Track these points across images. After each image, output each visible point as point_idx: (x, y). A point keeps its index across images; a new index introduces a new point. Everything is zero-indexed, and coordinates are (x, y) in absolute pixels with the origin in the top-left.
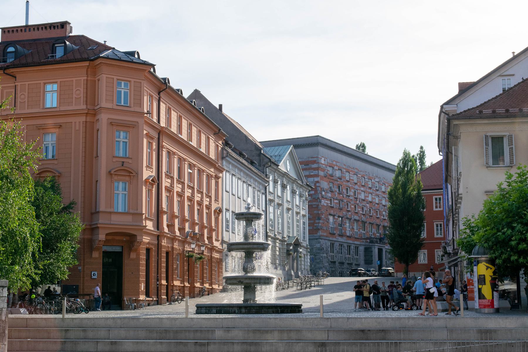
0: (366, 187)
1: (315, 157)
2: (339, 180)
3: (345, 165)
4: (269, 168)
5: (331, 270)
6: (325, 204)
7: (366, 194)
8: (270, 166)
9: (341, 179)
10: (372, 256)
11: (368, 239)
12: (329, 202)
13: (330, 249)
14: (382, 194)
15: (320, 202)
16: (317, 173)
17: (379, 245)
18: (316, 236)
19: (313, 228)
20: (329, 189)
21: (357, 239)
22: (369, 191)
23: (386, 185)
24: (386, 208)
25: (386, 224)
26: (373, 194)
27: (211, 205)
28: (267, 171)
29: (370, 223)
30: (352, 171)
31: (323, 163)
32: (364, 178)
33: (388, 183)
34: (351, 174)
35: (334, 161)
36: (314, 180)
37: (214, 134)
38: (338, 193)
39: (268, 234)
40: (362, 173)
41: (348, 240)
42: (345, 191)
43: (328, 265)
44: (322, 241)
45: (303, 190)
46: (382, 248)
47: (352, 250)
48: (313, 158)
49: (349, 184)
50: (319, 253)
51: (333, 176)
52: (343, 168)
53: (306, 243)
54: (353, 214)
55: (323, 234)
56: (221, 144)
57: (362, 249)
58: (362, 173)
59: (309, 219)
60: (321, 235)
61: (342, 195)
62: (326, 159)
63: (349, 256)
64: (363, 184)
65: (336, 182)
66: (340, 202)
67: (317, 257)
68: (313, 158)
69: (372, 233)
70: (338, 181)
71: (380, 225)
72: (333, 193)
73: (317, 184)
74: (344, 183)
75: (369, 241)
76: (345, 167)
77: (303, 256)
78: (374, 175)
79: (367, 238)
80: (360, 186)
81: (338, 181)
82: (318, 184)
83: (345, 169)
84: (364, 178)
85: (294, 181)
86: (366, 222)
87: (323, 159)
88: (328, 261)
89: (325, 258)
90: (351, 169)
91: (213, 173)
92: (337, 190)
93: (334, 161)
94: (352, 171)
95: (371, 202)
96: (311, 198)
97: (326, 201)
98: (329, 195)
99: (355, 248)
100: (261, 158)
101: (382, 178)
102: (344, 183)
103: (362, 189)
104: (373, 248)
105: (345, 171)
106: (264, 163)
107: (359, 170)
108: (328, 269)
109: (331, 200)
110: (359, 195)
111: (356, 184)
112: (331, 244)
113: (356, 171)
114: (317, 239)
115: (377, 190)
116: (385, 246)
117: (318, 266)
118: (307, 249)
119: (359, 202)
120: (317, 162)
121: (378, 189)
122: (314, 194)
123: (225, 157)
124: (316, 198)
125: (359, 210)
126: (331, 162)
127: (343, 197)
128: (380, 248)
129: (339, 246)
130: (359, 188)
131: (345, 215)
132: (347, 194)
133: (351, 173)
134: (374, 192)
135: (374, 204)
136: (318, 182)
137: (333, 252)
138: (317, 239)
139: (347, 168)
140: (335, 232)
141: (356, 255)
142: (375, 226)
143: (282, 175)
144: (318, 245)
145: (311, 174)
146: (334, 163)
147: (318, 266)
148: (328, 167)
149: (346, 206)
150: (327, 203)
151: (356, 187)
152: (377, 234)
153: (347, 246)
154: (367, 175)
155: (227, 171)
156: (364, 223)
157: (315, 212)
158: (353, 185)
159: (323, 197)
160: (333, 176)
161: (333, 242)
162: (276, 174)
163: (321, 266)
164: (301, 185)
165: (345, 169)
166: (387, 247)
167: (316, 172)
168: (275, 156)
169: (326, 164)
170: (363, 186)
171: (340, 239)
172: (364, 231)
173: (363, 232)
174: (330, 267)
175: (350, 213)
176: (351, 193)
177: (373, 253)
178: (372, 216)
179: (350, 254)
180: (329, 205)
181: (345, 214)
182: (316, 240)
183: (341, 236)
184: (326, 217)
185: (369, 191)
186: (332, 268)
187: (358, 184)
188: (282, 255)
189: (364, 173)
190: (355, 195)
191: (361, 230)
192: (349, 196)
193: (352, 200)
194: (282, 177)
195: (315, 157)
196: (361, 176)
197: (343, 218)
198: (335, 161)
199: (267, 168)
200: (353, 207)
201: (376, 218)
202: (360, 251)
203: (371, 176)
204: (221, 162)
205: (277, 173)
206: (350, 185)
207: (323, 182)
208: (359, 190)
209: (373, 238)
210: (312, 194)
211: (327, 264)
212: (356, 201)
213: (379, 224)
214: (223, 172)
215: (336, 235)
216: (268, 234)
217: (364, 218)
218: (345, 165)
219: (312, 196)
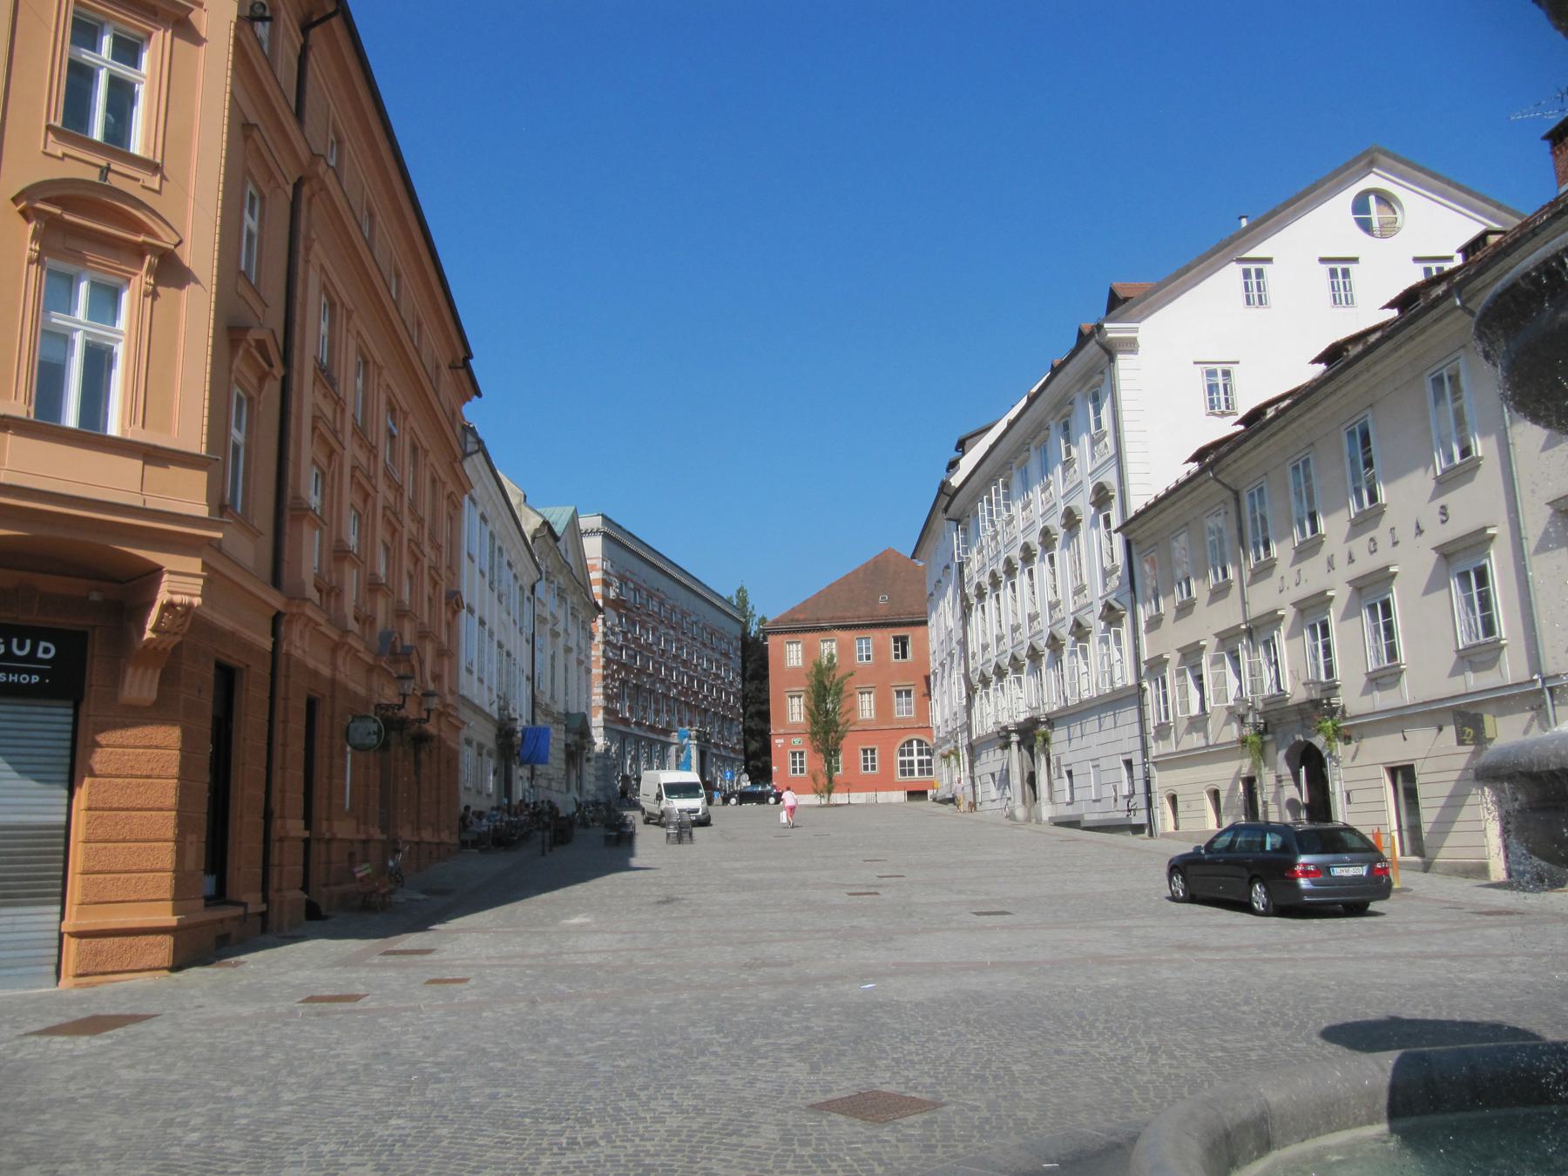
40: (671, 602)
52: (642, 587)
76: (645, 585)
94: (658, 597)
105: (645, 593)
113: (663, 596)
115: (695, 639)
146: (628, 574)
165: (646, 589)
203: (685, 608)
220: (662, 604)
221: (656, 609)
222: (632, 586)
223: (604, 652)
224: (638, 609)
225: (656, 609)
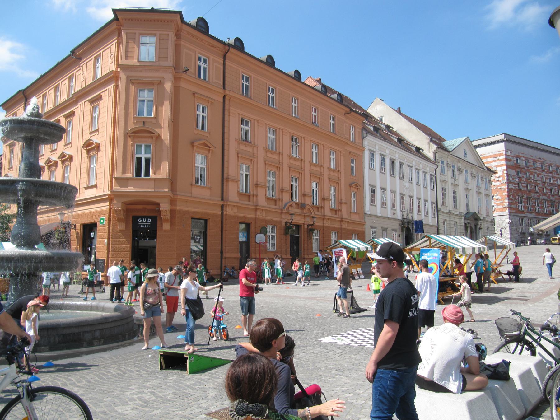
2: (526, 168)
3: (531, 156)
6: (513, 188)
12: (517, 186)
22: (557, 176)
38: (525, 179)
40: (549, 162)
51: (520, 165)
65: (523, 170)
66: (527, 185)
74: (531, 170)
76: (531, 158)
90: (537, 159)
92: (525, 176)
98: (517, 180)
102: (531, 170)
103: (550, 175)
109: (518, 184)
112: (520, 219)
125: (548, 191)
149: (534, 189)
150: (515, 187)
151: (544, 173)
156: (553, 202)
161: (522, 218)
165: (532, 159)
171: (529, 215)
172: (553, 208)
183: (530, 212)
185: (557, 176)
191: (550, 208)
193: (539, 184)
206: (538, 172)
208: (547, 176)
212: (544, 184)
215: (525, 211)
217: (552, 198)
218: (531, 156)
220: (542, 164)
222: (524, 159)
223: (508, 186)
224: (528, 167)
225: (539, 166)
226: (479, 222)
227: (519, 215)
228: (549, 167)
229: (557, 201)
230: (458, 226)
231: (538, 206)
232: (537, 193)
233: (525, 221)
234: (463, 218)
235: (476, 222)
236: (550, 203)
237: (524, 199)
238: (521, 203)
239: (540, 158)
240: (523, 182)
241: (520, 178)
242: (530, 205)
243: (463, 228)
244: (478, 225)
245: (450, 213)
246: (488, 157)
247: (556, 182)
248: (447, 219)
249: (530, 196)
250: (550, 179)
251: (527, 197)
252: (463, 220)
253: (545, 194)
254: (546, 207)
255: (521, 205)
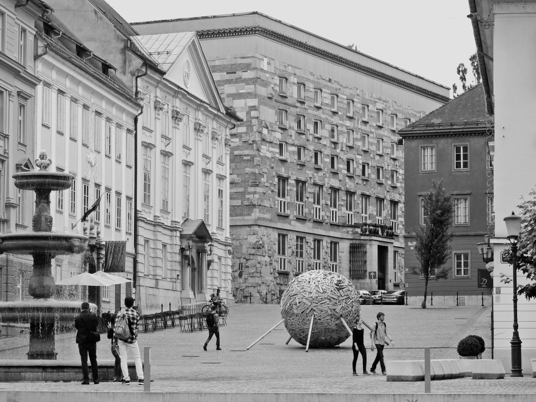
0: (356, 121)
1: (249, 57)
2: (298, 105)
3: (311, 74)
4: (144, 77)
5: (278, 289)
6: (269, 155)
7: (357, 134)
8: (145, 74)
9: (303, 103)
10: (365, 262)
11: (358, 227)
12: (277, 150)
13: (276, 246)
14: (390, 135)
15: (258, 150)
16: (253, 91)
17: (380, 239)
18: (248, 220)
19: (242, 203)
20: (278, 124)
21: (336, 227)
23: (400, 116)
24: (397, 163)
25: (397, 198)
26: (371, 135)
27: (8, 154)
28: (139, 84)
29: (363, 195)
30: (326, 87)
31: (265, 69)
32: (353, 101)
33: (403, 113)
34: (325, 92)
35: (288, 65)
36: (246, 104)
37: (17, 6)
39: (139, 215)
41: (317, 228)
42: (311, 127)
43: (273, 280)
44: (261, 231)
45: (220, 124)
46: (386, 245)
47: (323, 248)
48: (245, 58)
49: (319, 113)
50: (253, 254)
51: (286, 97)
52: (308, 80)
53: (224, 235)
54: (328, 175)
55: (262, 216)
56: (33, 27)
57: (344, 247)
58: (347, 90)
59: (231, 183)
60: (259, 219)
61: (304, 137)
62: (272, 62)
63: (318, 262)
64: (351, 115)
65: (292, 109)
67: (249, 263)
68: (245, 58)
69: (367, 216)
70: (297, 107)
71: (385, 197)
72: (286, 132)
73: (254, 113)
75: (359, 230)
76: (311, 78)
77: (216, 259)
78: (374, 95)
79: (356, 226)
80: (344, 117)
81: (297, 107)
82: (255, 112)
83: (313, 82)
84: (353, 101)
85: (199, 104)
86: (354, 193)
87: (266, 60)
88: (272, 271)
89: (266, 265)
91: (12, 88)
92: (295, 125)
93: (288, 65)
94: (326, 87)
95: (365, 152)
96: (240, 140)
97: (271, 149)
98: (278, 135)
99: (329, 245)
100: (127, 56)
101: (390, 101)
102: (309, 111)
103: (348, 123)
104: (368, 246)
106: (132, 68)
107: (341, 85)
108: (273, 288)
109: (281, 146)
110: (341, 136)
111: (335, 113)
114: (250, 226)
115: (380, 127)
116: (392, 241)
117: (251, 281)
118: (225, 245)
119: (342, 150)
120: (253, 66)
121: (380, 124)
122: (246, 133)
123: (41, 55)
124: (250, 142)
125: (341, 166)
126: (282, 68)
127: (308, 140)
128: (383, 245)
129: (297, 241)
130: (341, 122)
131: (310, 178)
132: (316, 135)
133: (324, 90)
134: (373, 130)
135: (372, 156)
136: (254, 108)
137: (284, 254)
138: (250, 226)
139: (316, 80)
140: (288, 212)
141: (331, 260)
142: (373, 200)
143: (173, 94)
144: (253, 239)
145: (241, 92)
146: (290, 69)
147: (251, 281)
148: (276, 78)
149: (313, 159)
151: (335, 120)
152: (377, 218)
153: (315, 240)
154: (358, 95)
155: (47, 85)
156: (350, 194)
157: (248, 170)
158: (330, 116)
159: (264, 140)
160: (286, 97)
161: (285, 232)
162: (158, 90)
163: (258, 280)
164: (215, 115)
165: (313, 82)
166: (396, 244)
167: (250, 88)
168: (159, 53)
169: (273, 71)
170: (351, 118)
173: (348, 212)
174: (277, 284)
175: (321, 174)
176: (323, 132)
177: (368, 254)
178: (367, 181)
179: (319, 258)
180: (278, 156)
181: (310, 176)
182: (247, 229)
183: (301, 220)
184: (270, 181)
185: (363, 127)
186: (282, 285)
187: (340, 113)
188: (169, 259)
189: (352, 92)
190: (333, 137)
191: (344, 209)
192: (319, 139)
194: (173, 96)
195: (249, 57)
196: (345, 97)
197: (307, 184)
198: (291, 66)
199: (138, 79)
200: (328, 160)
201: (376, 185)
202: (341, 250)
203: (367, 97)
204: (32, 65)
205: (161, 89)
206: (323, 116)
207: (266, 108)
208: (342, 125)
209: (369, 225)
210: (242, 133)
211: (269, 278)
212: (335, 148)
213: (382, 196)
214: (36, 85)
215: (291, 217)
216: (139, 215)
217: (350, 185)
218: (311, 74)
219: (241, 137)
220: (335, 95)
221: (328, 101)
224: (303, 103)
225: (328, 101)
226: (206, 245)
227: (279, 225)
228: (348, 104)
229: (359, 192)
230: (168, 255)
231: (318, 203)
232: (319, 169)
233: (291, 241)
234: (178, 234)
235: (200, 244)
236: (344, 198)
237: (291, 184)
238: (284, 196)
239: (330, 80)
240: (290, 141)
241: (284, 129)
242: (302, 200)
243: (178, 258)
244: (205, 251)
245: (156, 224)
246: (220, 69)
247: (360, 143)
248: (149, 235)
249: (303, 179)
250: (348, 133)
251: (298, 181)
252: (177, 241)
253: (335, 174)
254: (335, 206)
255: (283, 200)
